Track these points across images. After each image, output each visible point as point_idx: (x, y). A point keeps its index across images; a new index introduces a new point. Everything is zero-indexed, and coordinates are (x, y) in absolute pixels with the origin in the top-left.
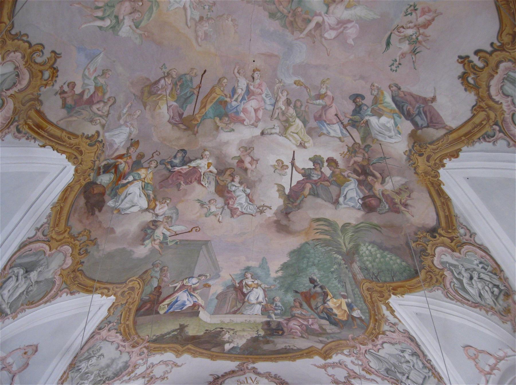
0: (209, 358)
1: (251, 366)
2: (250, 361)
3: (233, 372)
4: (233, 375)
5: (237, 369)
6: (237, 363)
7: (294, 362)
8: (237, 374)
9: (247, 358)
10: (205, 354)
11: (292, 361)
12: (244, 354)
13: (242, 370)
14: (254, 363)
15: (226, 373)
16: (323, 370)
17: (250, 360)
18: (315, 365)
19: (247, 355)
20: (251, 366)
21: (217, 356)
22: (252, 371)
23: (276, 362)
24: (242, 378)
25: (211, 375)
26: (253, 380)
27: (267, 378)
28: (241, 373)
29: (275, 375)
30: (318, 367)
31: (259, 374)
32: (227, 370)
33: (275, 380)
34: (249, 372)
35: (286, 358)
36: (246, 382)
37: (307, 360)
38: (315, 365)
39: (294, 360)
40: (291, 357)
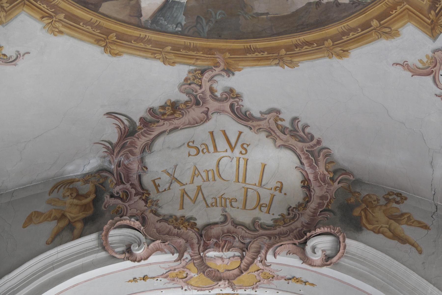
0: (98, 42)
1: (222, 83)
2: (217, 65)
3: (174, 108)
4: (176, 122)
5: (184, 98)
6: (181, 71)
7: (344, 62)
8: (186, 119)
9: (210, 51)
10: (87, 23)
11: (340, 56)
12: (198, 35)
13: (197, 103)
14: (229, 71)
15: (151, 111)
16: (429, 79)
17: (220, 58)
18: (405, 65)
19: (209, 36)
20: (222, 83)
21: (121, 37)
22: (227, 106)
23: (292, 65)
24: (200, 133)
25: (109, 114)
26: (233, 141)
27: (270, 133)
28: (196, 113)
29: (295, 119)
30: (416, 72)
31: (244, 117)
32: (157, 100)
33: (293, 142)
34: (219, 111)
35: (317, 48)
36: (211, 148)
37: (383, 44)
38: (405, 65)
39: (343, 53)
40: (335, 38)
